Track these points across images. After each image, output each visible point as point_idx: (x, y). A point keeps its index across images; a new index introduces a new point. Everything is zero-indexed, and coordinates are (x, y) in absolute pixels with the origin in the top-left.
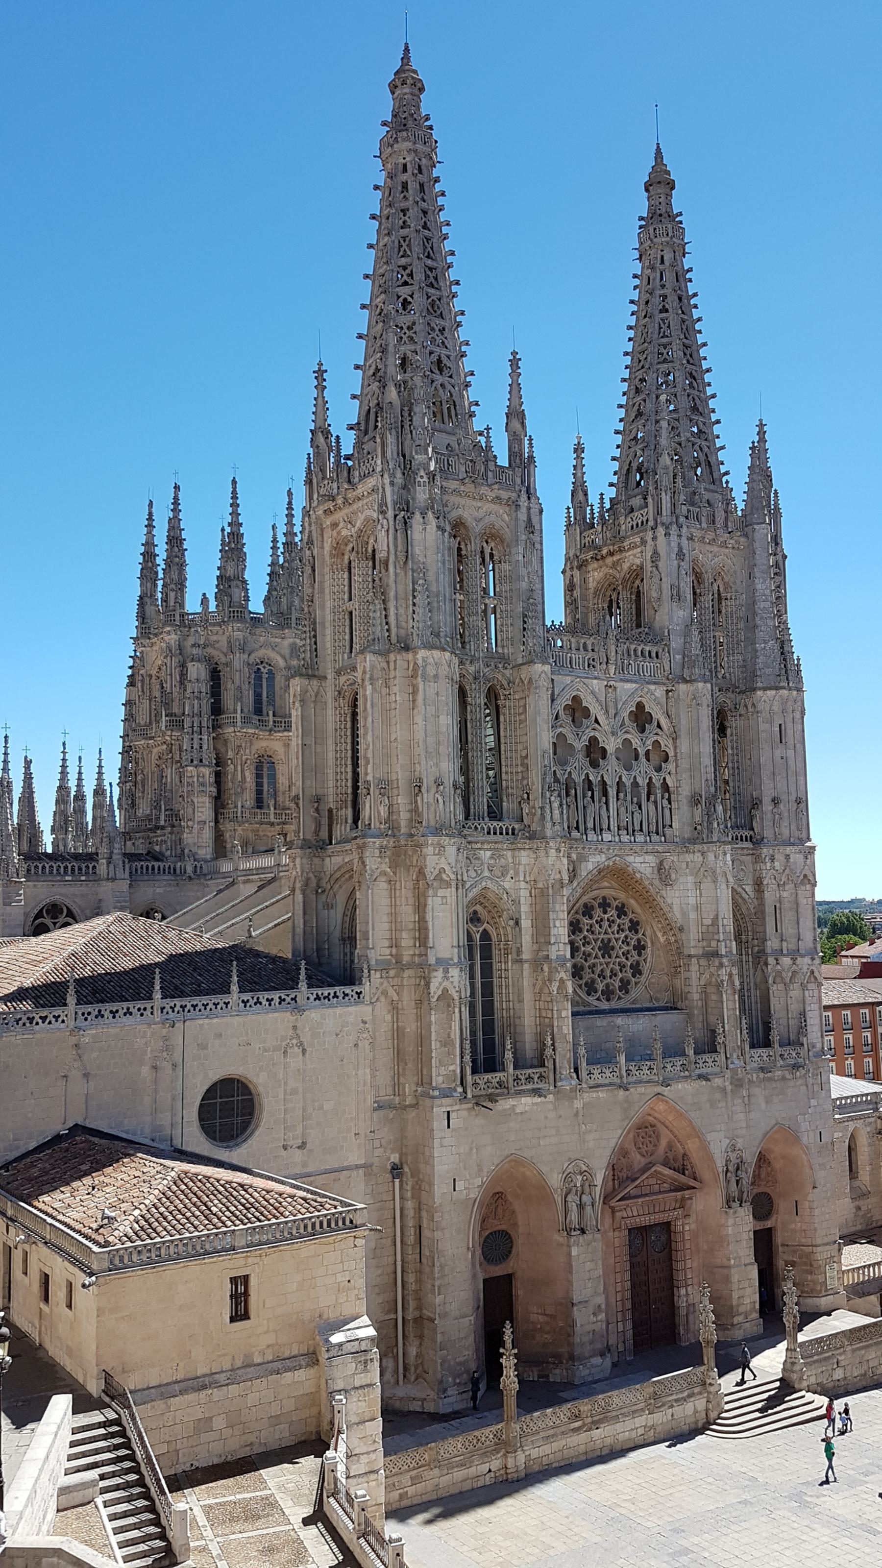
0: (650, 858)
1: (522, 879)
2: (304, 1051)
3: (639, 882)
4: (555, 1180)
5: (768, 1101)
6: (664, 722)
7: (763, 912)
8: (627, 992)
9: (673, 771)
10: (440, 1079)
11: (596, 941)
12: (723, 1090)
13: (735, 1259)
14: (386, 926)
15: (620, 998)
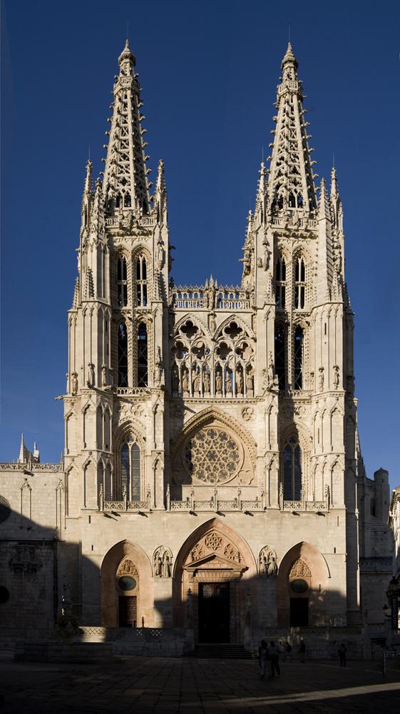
0: (235, 406)
5: (296, 528)
9: (255, 358)
11: (205, 452)
12: (263, 520)
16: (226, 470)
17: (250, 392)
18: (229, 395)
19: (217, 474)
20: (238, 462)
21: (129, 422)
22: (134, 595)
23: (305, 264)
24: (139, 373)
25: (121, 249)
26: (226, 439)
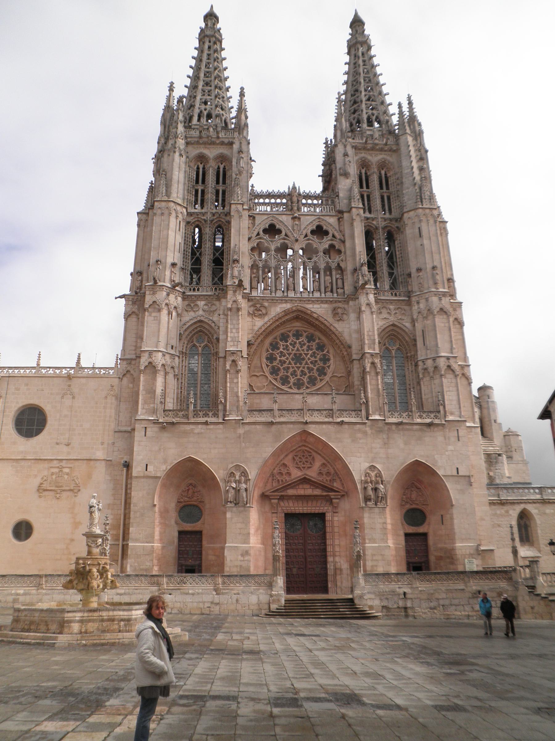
0: (326, 306)
1: (221, 313)
2: (73, 398)
3: (317, 319)
4: (219, 475)
5: (406, 443)
6: (336, 234)
7: (415, 335)
8: (314, 385)
9: (344, 259)
10: (144, 411)
11: (290, 354)
12: (365, 433)
13: (370, 540)
14: (134, 339)
15: (307, 388)
16: (316, 374)
17: (340, 291)
18: (317, 295)
19: (305, 380)
20: (329, 367)
21: (201, 321)
22: (197, 529)
23: (388, 175)
24: (213, 273)
25: (202, 158)
26: (314, 341)
